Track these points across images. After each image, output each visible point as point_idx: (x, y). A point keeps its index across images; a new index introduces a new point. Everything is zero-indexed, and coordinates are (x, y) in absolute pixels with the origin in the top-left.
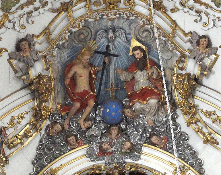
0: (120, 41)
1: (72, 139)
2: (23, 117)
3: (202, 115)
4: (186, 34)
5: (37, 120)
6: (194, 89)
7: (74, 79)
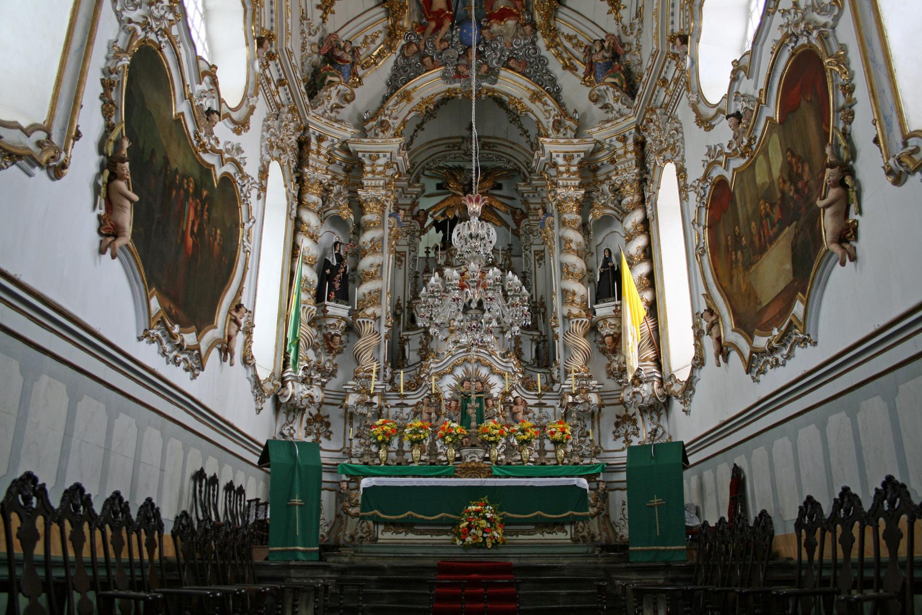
1: (427, 59)
2: (377, 37)
3: (563, 39)
5: (392, 40)
6: (556, 10)
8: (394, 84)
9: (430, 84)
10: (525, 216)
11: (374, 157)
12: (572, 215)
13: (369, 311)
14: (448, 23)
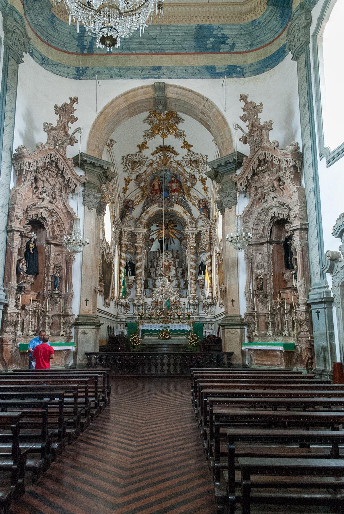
0: (168, 173)
4: (188, 173)
7: (154, 185)
8: (144, 209)
9: (154, 209)
10: (183, 239)
11: (139, 234)
12: (193, 251)
13: (139, 278)
14: (159, 193)
